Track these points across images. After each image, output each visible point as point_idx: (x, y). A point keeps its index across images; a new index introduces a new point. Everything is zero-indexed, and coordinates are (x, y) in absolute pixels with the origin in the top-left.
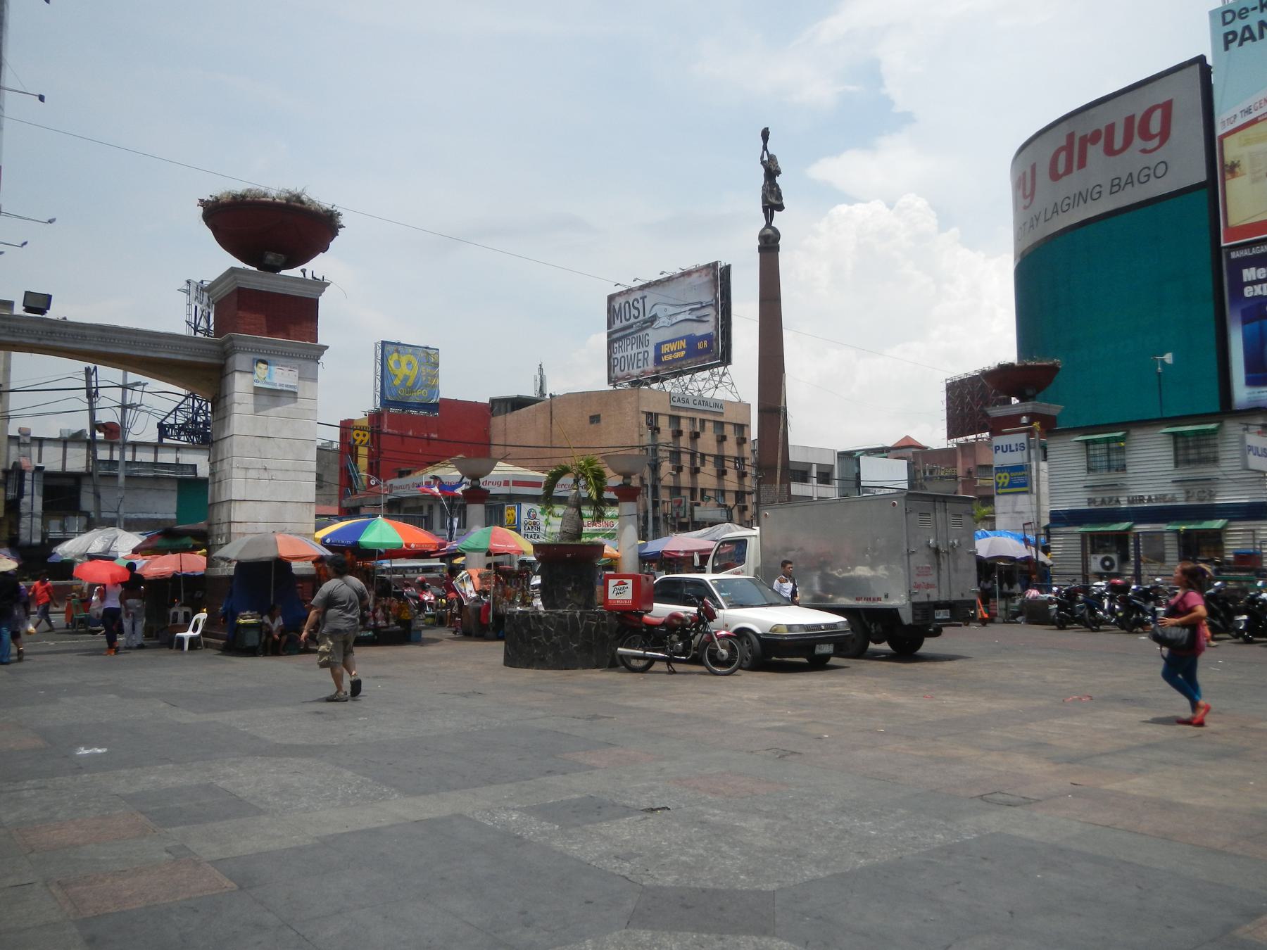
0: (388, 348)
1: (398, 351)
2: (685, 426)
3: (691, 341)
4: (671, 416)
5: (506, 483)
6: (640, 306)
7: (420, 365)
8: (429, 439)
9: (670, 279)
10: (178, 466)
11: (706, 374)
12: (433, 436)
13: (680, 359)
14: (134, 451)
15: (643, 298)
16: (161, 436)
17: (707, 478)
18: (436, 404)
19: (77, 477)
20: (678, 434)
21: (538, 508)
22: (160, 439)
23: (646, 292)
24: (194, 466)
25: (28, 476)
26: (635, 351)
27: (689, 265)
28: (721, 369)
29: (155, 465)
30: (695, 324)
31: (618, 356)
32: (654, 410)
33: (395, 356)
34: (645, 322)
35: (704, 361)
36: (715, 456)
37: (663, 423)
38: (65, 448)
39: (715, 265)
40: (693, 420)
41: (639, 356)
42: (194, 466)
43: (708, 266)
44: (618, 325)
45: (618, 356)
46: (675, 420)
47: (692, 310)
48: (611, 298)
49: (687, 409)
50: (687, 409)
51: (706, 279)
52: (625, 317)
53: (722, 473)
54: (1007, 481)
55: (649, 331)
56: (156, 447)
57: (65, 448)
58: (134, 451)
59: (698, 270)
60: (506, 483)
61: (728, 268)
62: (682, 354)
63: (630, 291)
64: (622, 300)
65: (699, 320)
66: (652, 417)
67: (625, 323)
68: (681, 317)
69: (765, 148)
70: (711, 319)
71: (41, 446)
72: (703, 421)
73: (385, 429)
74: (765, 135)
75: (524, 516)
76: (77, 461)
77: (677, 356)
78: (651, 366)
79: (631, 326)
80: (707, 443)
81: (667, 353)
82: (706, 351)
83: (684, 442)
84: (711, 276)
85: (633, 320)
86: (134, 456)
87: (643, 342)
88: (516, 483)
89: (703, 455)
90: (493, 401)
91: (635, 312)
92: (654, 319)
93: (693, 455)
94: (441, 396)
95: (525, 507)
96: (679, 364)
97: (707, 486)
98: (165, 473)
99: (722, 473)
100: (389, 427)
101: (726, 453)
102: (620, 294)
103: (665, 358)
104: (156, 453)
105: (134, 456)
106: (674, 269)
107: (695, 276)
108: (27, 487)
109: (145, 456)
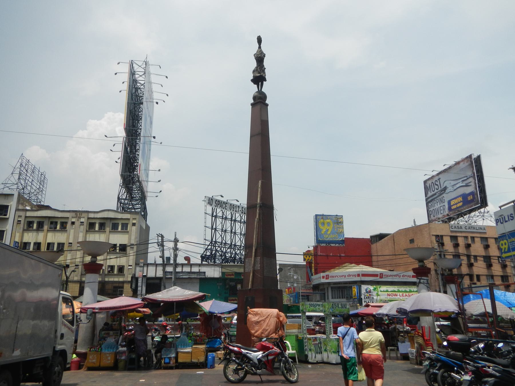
0: (318, 217)
1: (322, 218)
2: (461, 241)
3: (464, 196)
4: (452, 237)
5: (359, 275)
6: (438, 183)
7: (334, 223)
8: (340, 256)
9: (450, 168)
10: (199, 273)
11: (477, 213)
12: (342, 255)
13: (460, 207)
14: (182, 267)
15: (439, 179)
16: (202, 261)
17: (480, 268)
18: (342, 241)
19: (160, 279)
20: (456, 246)
21: (371, 288)
22: (202, 262)
23: (440, 176)
24: (205, 272)
25: (140, 280)
26: (439, 206)
27: (458, 159)
28: (482, 210)
29: (191, 273)
30: (465, 188)
31: (431, 209)
32: (440, 234)
33: (322, 220)
34: (441, 191)
35: (472, 206)
36: (484, 257)
37: (447, 241)
38: (156, 267)
39: (470, 156)
40: (466, 237)
41: (442, 208)
42: (205, 272)
43: (467, 158)
44: (430, 194)
45: (431, 209)
46: (454, 238)
47: (463, 181)
48: (425, 182)
49: (461, 232)
50: (461, 232)
51: (467, 164)
52: (433, 189)
53: (489, 266)
54: (507, 246)
55: (444, 195)
56: (199, 265)
57: (156, 267)
58: (182, 267)
59: (463, 160)
60: (359, 275)
61: (479, 157)
62: (461, 204)
63: (433, 177)
64: (430, 182)
65: (467, 186)
66: (439, 239)
67: (433, 193)
68: (458, 186)
69: (260, 47)
70: (473, 184)
71: (147, 267)
72: (473, 238)
73: (319, 254)
74: (259, 40)
75: (363, 291)
76: (160, 273)
77: (459, 205)
78: (447, 212)
79: (435, 194)
80: (477, 249)
81: (454, 205)
82: (472, 201)
83: (462, 250)
84: (469, 162)
85: (436, 191)
86: (182, 269)
87: (442, 201)
88: (364, 275)
89: (475, 257)
90: (371, 237)
91: (436, 187)
92: (445, 188)
93: (469, 257)
94: (346, 236)
95: (364, 287)
96: (460, 209)
97: (480, 273)
98: (193, 276)
99: (489, 266)
100: (321, 252)
101: (491, 254)
102: (429, 179)
103: (453, 208)
104: (191, 267)
105: (182, 269)
106: (452, 163)
107: (462, 163)
108: (140, 284)
109: (195, 269)
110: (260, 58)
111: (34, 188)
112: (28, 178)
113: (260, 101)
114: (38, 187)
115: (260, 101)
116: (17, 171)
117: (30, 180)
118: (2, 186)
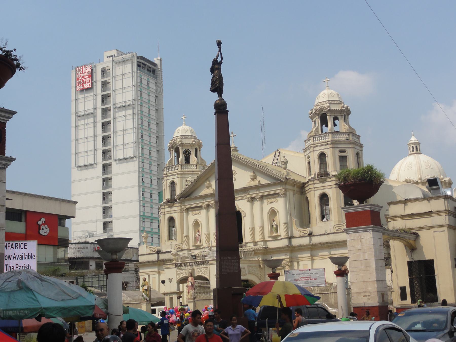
113: (221, 110)
115: (221, 110)
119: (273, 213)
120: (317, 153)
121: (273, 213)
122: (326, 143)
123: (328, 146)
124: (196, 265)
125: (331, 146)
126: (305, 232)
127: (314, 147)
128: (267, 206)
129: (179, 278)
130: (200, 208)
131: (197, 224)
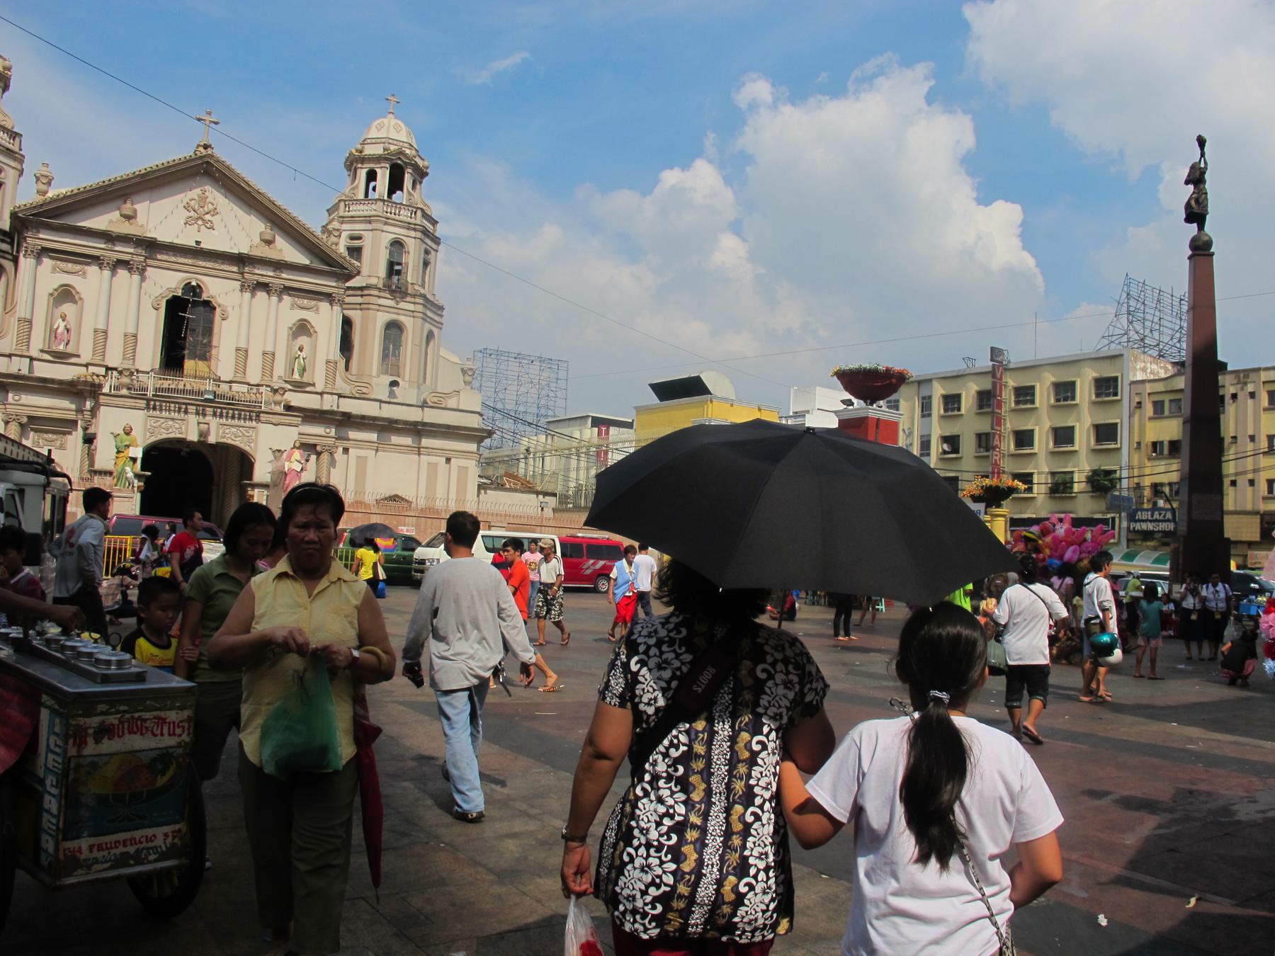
69: (1203, 155)
74: (1201, 142)
110: (1196, 177)
111: (1166, 330)
112: (1149, 317)
113: (1201, 250)
114: (1177, 327)
115: (1201, 250)
116: (1124, 309)
117: (1156, 319)
118: (1105, 342)
119: (302, 328)
120: (386, 239)
121: (302, 328)
122: (409, 226)
123: (413, 234)
124: (215, 415)
125: (419, 235)
126: (364, 390)
127: (386, 224)
128: (288, 311)
129: (153, 439)
130: (96, 260)
131: (65, 295)
